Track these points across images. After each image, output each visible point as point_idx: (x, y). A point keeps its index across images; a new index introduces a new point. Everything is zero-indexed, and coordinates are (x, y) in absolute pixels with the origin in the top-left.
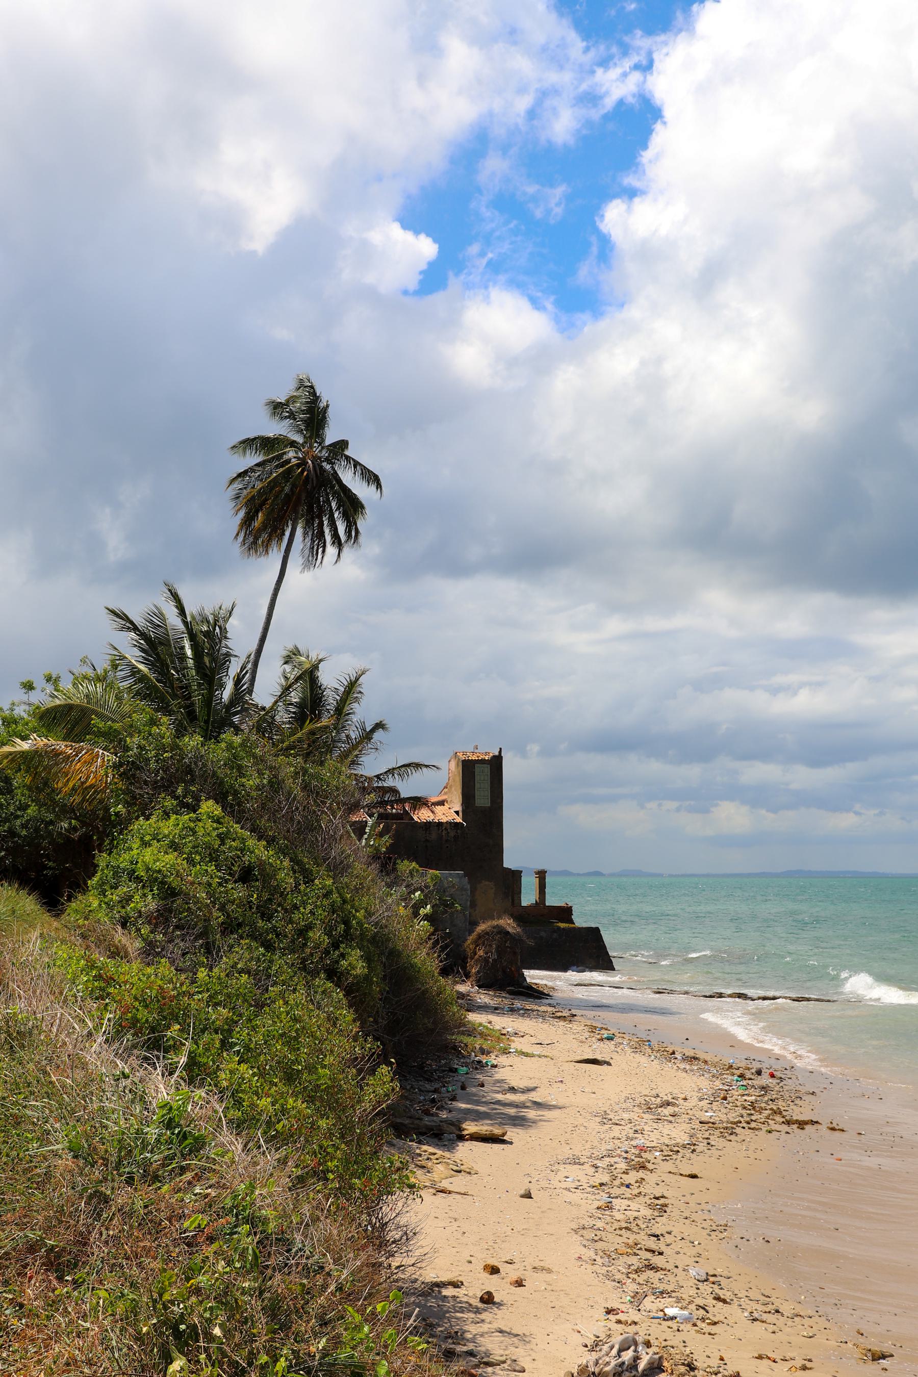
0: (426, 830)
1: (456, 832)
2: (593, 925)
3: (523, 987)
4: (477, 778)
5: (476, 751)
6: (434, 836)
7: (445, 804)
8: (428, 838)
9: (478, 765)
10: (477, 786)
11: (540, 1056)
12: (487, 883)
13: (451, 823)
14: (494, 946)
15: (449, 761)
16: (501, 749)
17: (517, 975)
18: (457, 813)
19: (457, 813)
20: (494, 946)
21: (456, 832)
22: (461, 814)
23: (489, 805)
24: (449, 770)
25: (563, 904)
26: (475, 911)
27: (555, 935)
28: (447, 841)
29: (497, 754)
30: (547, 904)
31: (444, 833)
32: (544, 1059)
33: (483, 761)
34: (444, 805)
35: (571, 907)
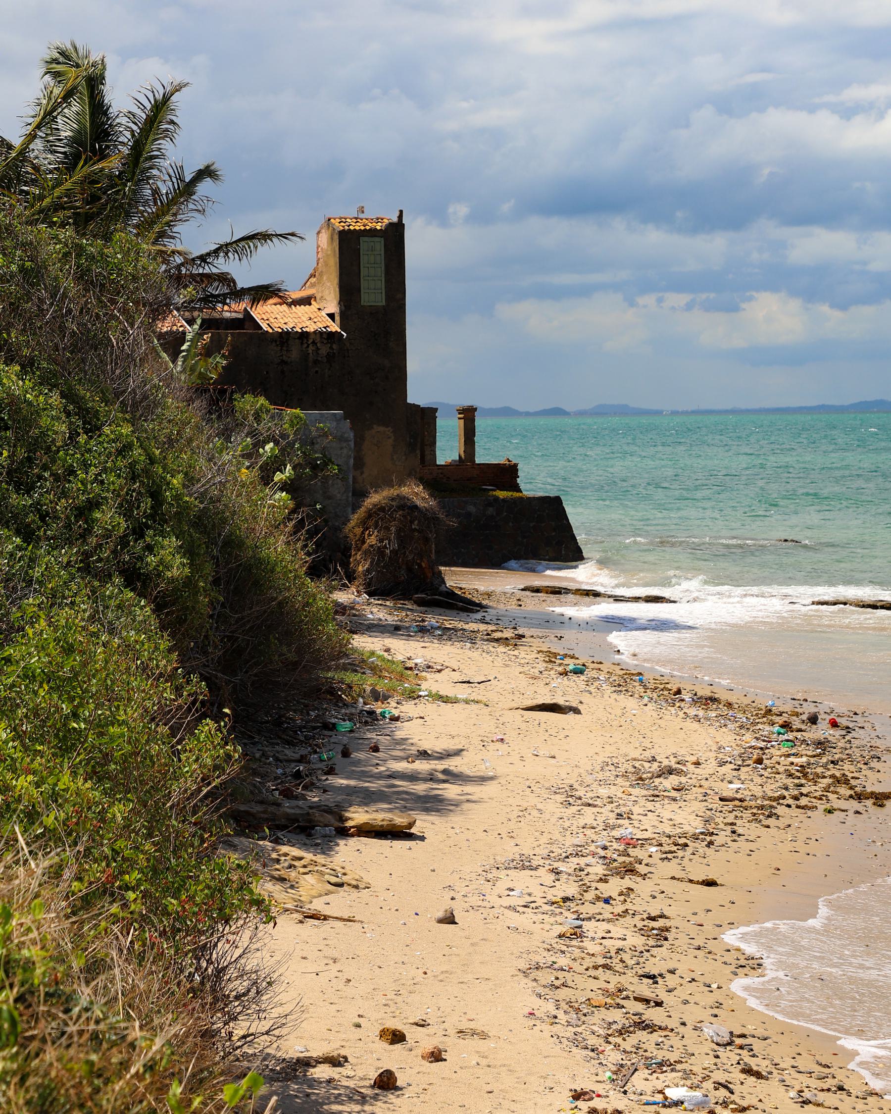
1: (331, 348)
2: (552, 494)
3: (441, 594)
4: (364, 259)
5: (361, 216)
6: (294, 354)
7: (313, 302)
9: (366, 239)
10: (363, 272)
11: (467, 702)
12: (381, 429)
13: (321, 333)
14: (393, 529)
15: (319, 233)
16: (401, 212)
17: (430, 575)
18: (331, 316)
19: (331, 316)
20: (393, 529)
22: (337, 318)
23: (384, 303)
24: (318, 247)
25: (502, 461)
26: (362, 473)
27: (491, 511)
28: (316, 362)
29: (395, 219)
30: (478, 461)
32: (474, 706)
33: (373, 232)
34: (310, 304)
35: (516, 465)
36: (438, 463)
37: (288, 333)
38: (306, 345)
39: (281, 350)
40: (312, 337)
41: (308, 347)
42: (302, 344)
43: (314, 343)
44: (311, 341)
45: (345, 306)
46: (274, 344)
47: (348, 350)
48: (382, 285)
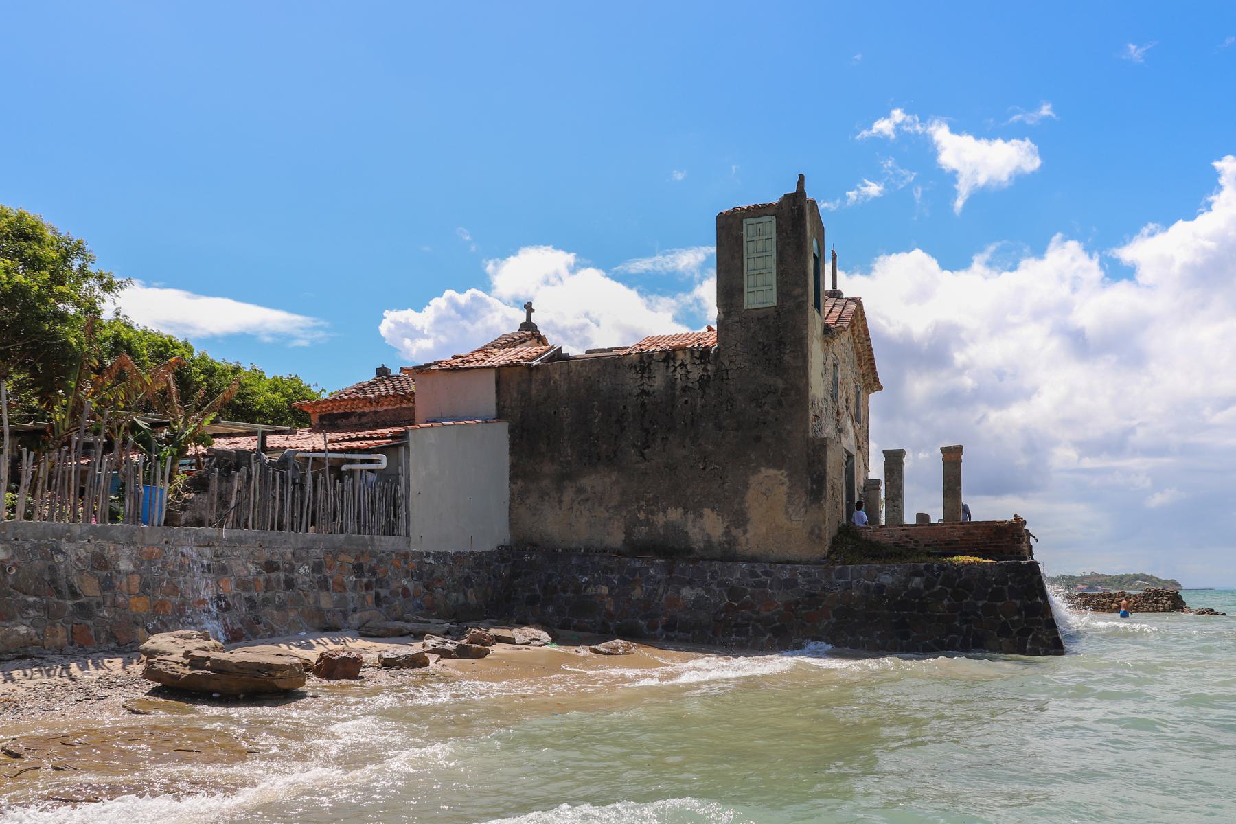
0: (643, 370)
1: (705, 370)
6: (658, 382)
8: (646, 388)
13: (692, 351)
21: (705, 370)
28: (685, 389)
31: (680, 371)
37: (650, 355)
38: (673, 368)
39: (642, 377)
40: (680, 355)
41: (675, 370)
43: (682, 364)
44: (678, 363)
45: (724, 313)
47: (727, 371)
48: (772, 279)
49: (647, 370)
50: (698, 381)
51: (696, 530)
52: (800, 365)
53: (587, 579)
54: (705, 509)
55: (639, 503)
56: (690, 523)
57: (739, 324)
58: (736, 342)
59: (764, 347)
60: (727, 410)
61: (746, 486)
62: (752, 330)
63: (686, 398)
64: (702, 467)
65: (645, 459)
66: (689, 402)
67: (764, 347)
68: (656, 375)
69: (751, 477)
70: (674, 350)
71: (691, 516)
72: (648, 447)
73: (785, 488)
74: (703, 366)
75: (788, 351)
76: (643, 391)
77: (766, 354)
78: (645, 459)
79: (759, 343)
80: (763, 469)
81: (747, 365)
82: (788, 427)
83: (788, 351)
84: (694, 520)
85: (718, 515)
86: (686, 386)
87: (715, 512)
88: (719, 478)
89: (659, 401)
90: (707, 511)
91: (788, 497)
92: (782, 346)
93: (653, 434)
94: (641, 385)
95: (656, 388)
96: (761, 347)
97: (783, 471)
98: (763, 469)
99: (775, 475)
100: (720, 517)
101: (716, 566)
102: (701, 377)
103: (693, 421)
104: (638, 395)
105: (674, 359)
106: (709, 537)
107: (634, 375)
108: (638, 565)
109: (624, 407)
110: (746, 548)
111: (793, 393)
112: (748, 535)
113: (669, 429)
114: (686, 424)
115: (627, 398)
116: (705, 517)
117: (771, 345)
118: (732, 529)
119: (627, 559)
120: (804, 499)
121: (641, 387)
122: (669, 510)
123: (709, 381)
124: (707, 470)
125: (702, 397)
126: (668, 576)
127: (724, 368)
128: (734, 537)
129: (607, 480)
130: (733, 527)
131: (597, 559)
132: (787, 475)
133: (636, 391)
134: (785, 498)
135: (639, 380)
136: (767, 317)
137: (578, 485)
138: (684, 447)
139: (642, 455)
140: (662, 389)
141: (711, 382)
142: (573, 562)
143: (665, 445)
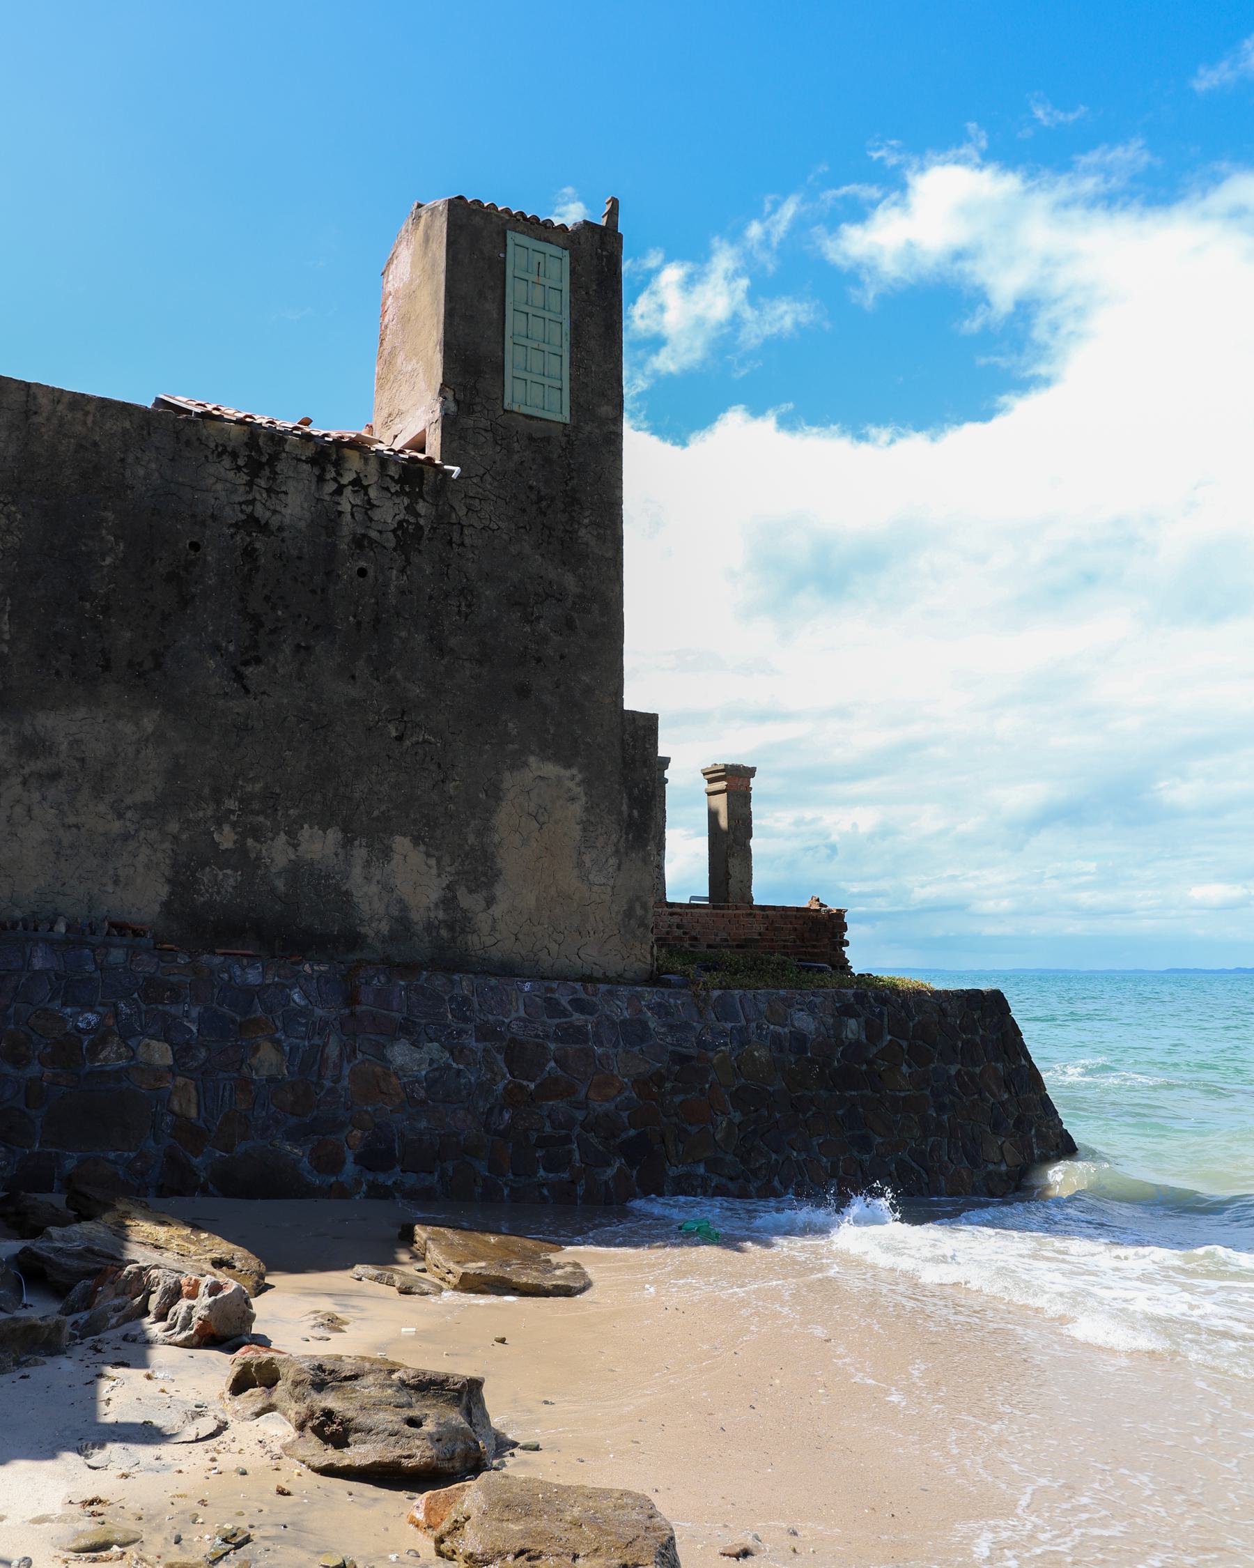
1: (410, 509)
4: (515, 292)
8: (259, 511)
10: (514, 323)
28: (360, 542)
31: (348, 501)
36: (669, 899)
37: (276, 437)
38: (332, 487)
39: (250, 484)
40: (354, 461)
41: (339, 491)
42: (321, 479)
43: (356, 482)
45: (457, 401)
46: (227, 462)
47: (462, 527)
49: (267, 472)
50: (394, 531)
51: (374, 889)
52: (609, 555)
53: (92, 1018)
54: (398, 839)
55: (219, 802)
56: (357, 871)
57: (489, 435)
58: (482, 471)
59: (540, 499)
60: (459, 611)
61: (495, 793)
62: (516, 457)
63: (363, 564)
64: (394, 734)
65: (247, 691)
66: (371, 573)
67: (540, 499)
68: (291, 486)
69: (507, 774)
70: (339, 443)
71: (360, 853)
72: (258, 661)
73: (577, 809)
74: (406, 501)
75: (586, 521)
76: (252, 520)
77: (545, 514)
78: (247, 691)
79: (531, 488)
80: (532, 760)
81: (503, 525)
82: (586, 679)
83: (586, 521)
84: (368, 864)
85: (428, 855)
86: (364, 536)
87: (422, 848)
88: (433, 767)
89: (295, 553)
90: (401, 843)
91: (584, 830)
92: (576, 508)
93: (272, 632)
94: (247, 503)
95: (287, 521)
96: (533, 497)
97: (574, 771)
98: (532, 760)
99: (559, 779)
100: (433, 862)
101: (465, 985)
102: (400, 523)
103: (377, 620)
104: (236, 525)
105: (339, 463)
106: (405, 909)
107: (231, 475)
108: (253, 976)
109: (195, 546)
110: (489, 941)
111: (595, 607)
112: (497, 910)
113: (317, 627)
114: (359, 623)
115: (203, 524)
116: (397, 858)
117: (553, 499)
118: (461, 893)
119: (218, 960)
120: (614, 838)
121: (249, 509)
122: (306, 832)
123: (420, 539)
124: (408, 743)
125: (403, 571)
126: (347, 1011)
127: (454, 519)
128: (465, 911)
129: (126, 728)
130: (463, 888)
131: (117, 955)
132: (583, 781)
133: (232, 515)
134: (577, 832)
135: (242, 489)
136: (547, 440)
137: (27, 730)
138: (353, 677)
139: (240, 677)
140: (302, 525)
141: (425, 542)
142: (38, 964)
143: (301, 664)
